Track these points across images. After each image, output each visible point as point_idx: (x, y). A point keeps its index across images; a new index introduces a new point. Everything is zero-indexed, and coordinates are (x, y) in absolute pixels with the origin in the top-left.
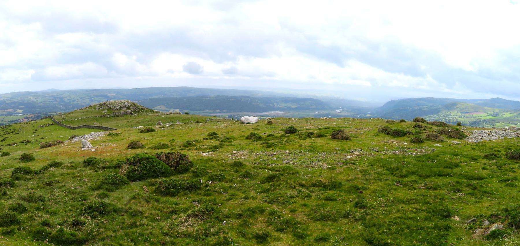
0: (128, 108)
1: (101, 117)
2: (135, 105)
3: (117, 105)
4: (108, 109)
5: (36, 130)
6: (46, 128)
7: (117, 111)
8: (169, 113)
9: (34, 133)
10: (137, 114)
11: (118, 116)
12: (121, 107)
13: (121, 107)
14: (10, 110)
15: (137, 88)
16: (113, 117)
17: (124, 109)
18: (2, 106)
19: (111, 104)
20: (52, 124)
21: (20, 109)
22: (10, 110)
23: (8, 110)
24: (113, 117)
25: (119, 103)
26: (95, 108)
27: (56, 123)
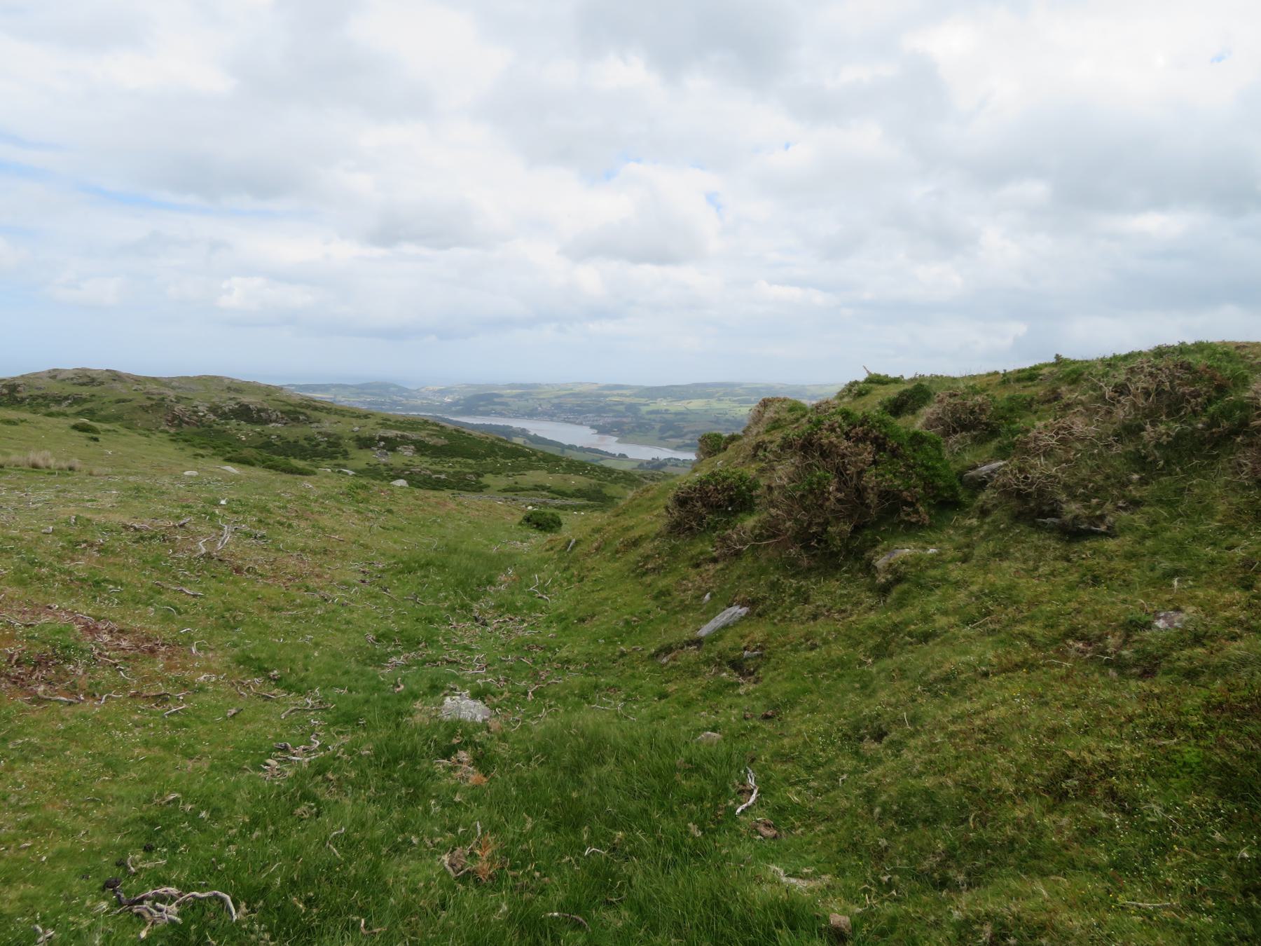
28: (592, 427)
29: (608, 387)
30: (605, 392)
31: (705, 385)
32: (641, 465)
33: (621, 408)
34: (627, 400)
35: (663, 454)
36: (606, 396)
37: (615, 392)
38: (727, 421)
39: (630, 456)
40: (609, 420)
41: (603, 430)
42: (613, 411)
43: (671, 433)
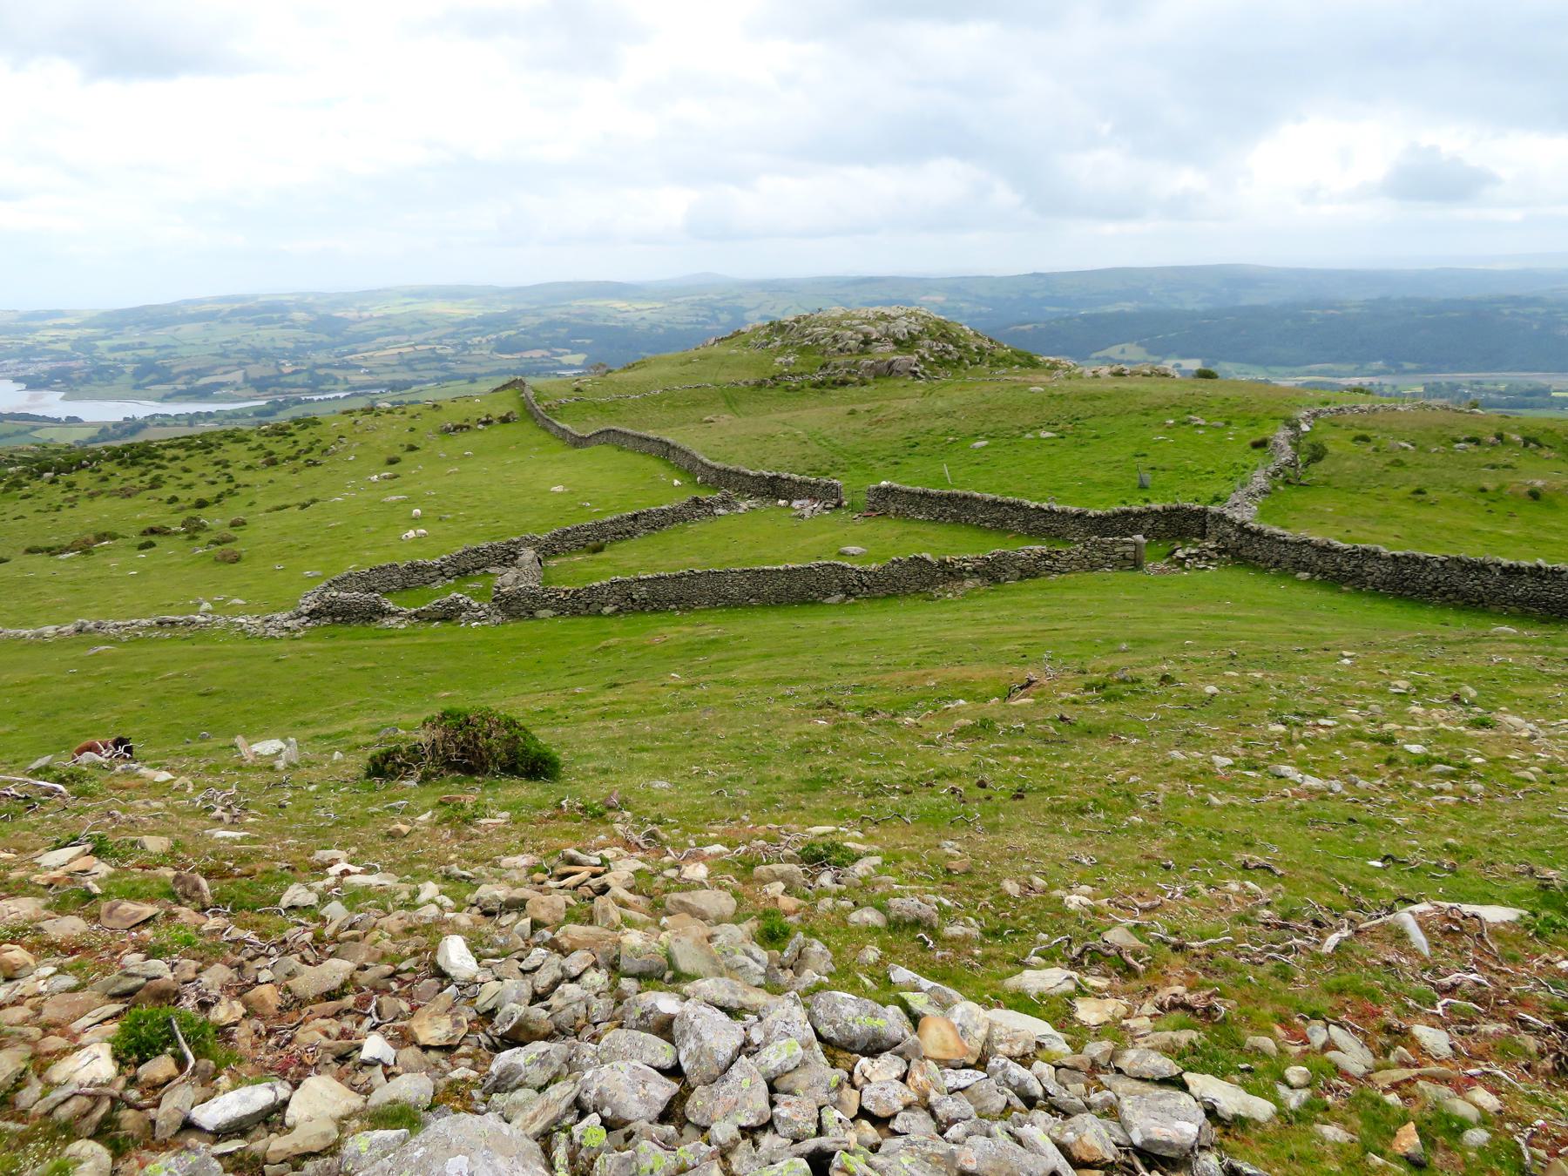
0: (905, 344)
1: (760, 385)
2: (943, 333)
3: (850, 327)
4: (803, 350)
5: (412, 448)
6: (463, 438)
7: (840, 360)
8: (1105, 370)
9: (392, 462)
10: (945, 375)
11: (844, 383)
12: (867, 342)
13: (867, 342)
14: (537, 354)
15: (1035, 275)
16: (815, 386)
17: (884, 352)
18: (504, 334)
19: (824, 323)
20: (505, 420)
21: (576, 350)
22: (537, 354)
23: (527, 355)
24: (815, 386)
25: (867, 320)
26: (746, 344)
27: (529, 413)
28: (17, 380)
29: (36, 316)
30: (30, 324)
31: (200, 302)
32: (105, 431)
33: (65, 347)
34: (73, 334)
35: (140, 409)
36: (34, 330)
37: (50, 323)
38: (240, 351)
39: (87, 418)
40: (45, 367)
41: (35, 384)
42: (52, 351)
43: (153, 377)
